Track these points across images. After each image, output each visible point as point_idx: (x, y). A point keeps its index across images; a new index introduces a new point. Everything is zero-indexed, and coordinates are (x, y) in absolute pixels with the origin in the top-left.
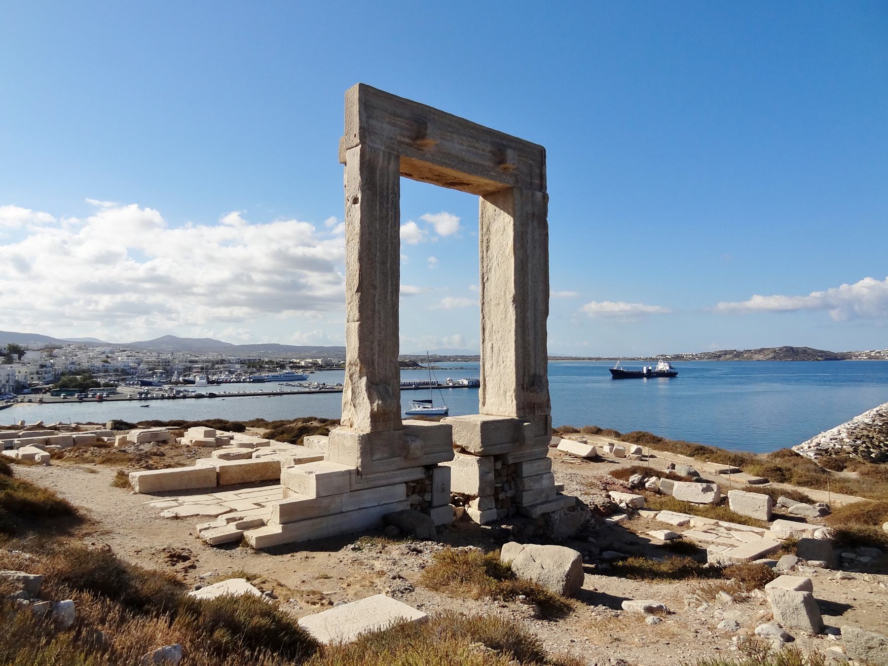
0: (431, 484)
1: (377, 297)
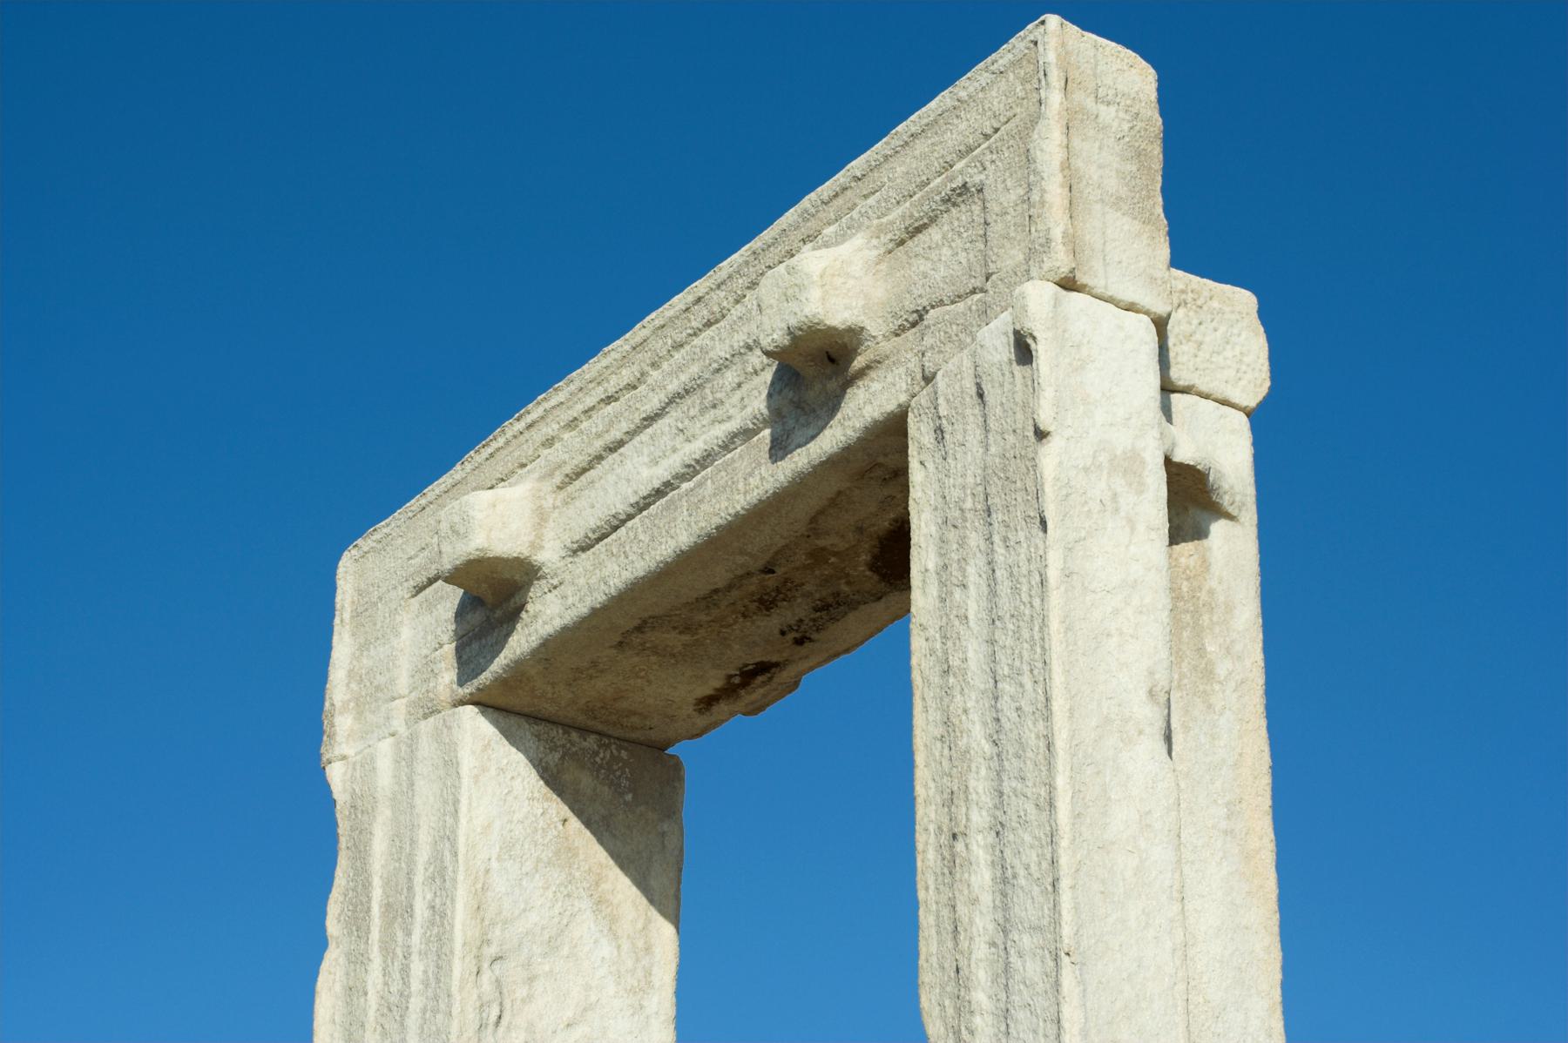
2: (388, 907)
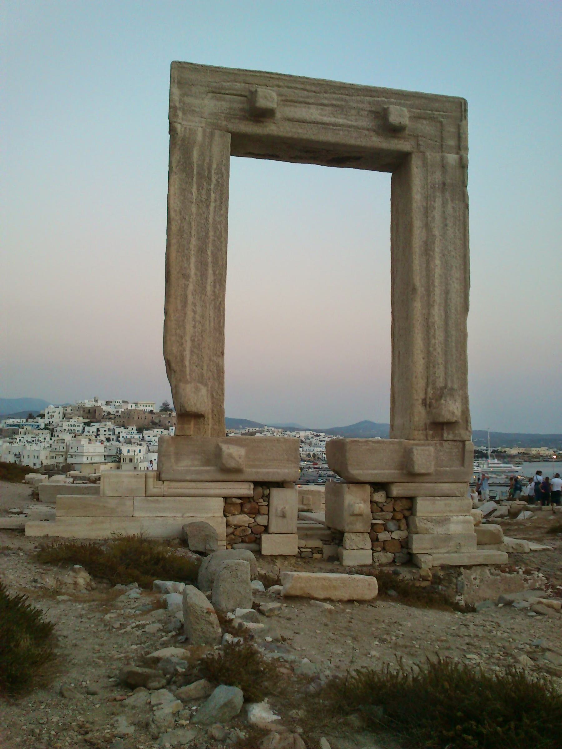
0: (268, 506)
1: (191, 287)
2: (198, 173)
